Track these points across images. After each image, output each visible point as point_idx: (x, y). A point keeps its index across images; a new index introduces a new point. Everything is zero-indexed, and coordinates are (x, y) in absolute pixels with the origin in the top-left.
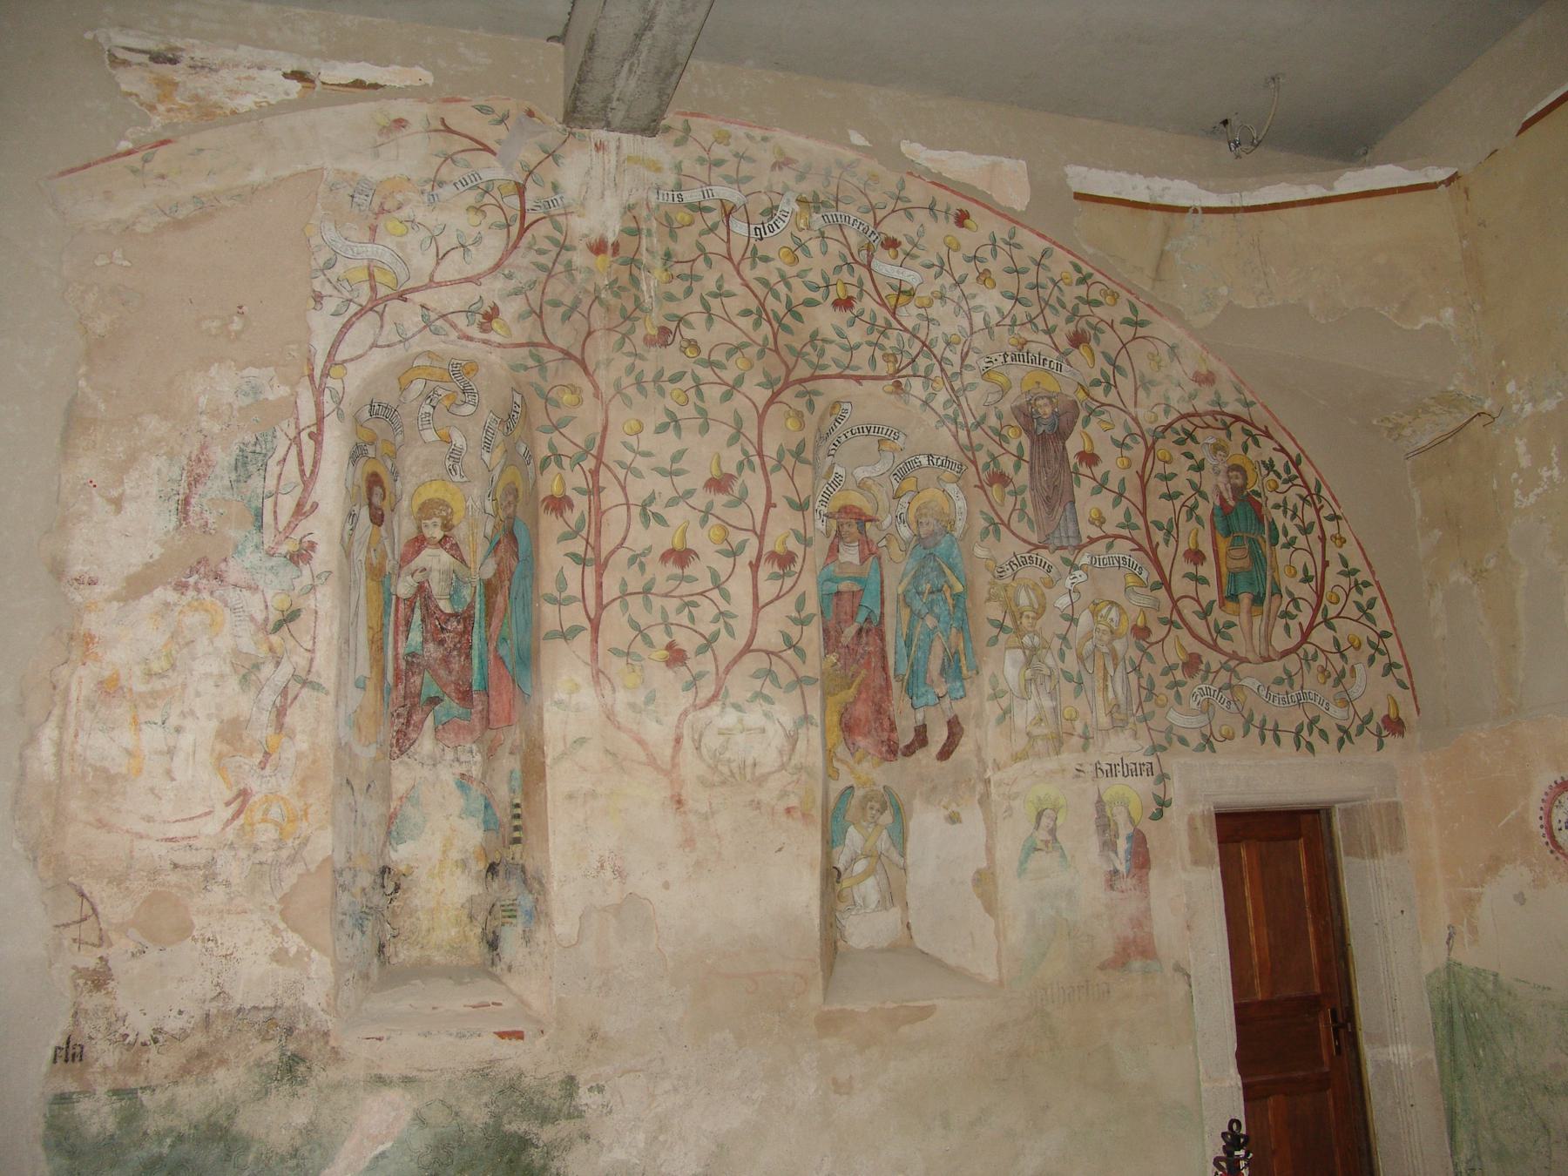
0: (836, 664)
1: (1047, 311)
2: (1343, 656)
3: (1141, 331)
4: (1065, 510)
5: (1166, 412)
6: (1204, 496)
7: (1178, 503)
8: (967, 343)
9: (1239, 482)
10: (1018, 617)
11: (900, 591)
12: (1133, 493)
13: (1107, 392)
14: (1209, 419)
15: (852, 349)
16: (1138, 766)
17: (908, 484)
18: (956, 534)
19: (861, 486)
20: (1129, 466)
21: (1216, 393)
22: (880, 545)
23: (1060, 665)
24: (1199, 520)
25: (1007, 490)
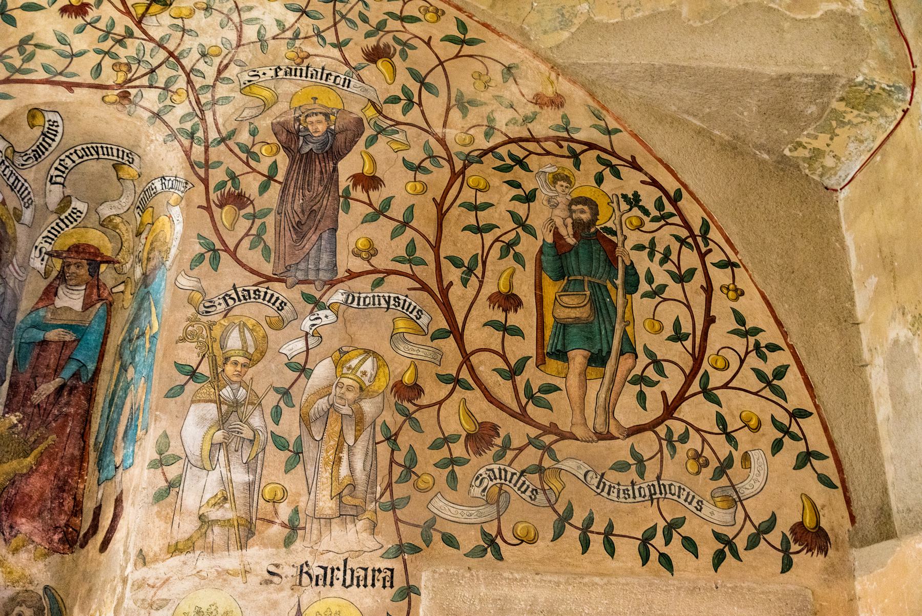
0: (16, 426)
1: (342, 26)
2: (730, 438)
3: (467, 50)
4: (320, 237)
5: (488, 135)
6: (530, 231)
7: (489, 238)
8: (230, 55)
9: (586, 217)
10: (220, 361)
11: (119, 343)
12: (424, 221)
13: (405, 111)
14: (550, 146)
15: (73, 56)
16: (370, 573)
17: (147, 218)
18: (168, 264)
19: (105, 224)
20: (424, 191)
21: (564, 117)
22: (114, 290)
23: (272, 427)
24: (518, 258)
25: (243, 212)
